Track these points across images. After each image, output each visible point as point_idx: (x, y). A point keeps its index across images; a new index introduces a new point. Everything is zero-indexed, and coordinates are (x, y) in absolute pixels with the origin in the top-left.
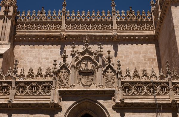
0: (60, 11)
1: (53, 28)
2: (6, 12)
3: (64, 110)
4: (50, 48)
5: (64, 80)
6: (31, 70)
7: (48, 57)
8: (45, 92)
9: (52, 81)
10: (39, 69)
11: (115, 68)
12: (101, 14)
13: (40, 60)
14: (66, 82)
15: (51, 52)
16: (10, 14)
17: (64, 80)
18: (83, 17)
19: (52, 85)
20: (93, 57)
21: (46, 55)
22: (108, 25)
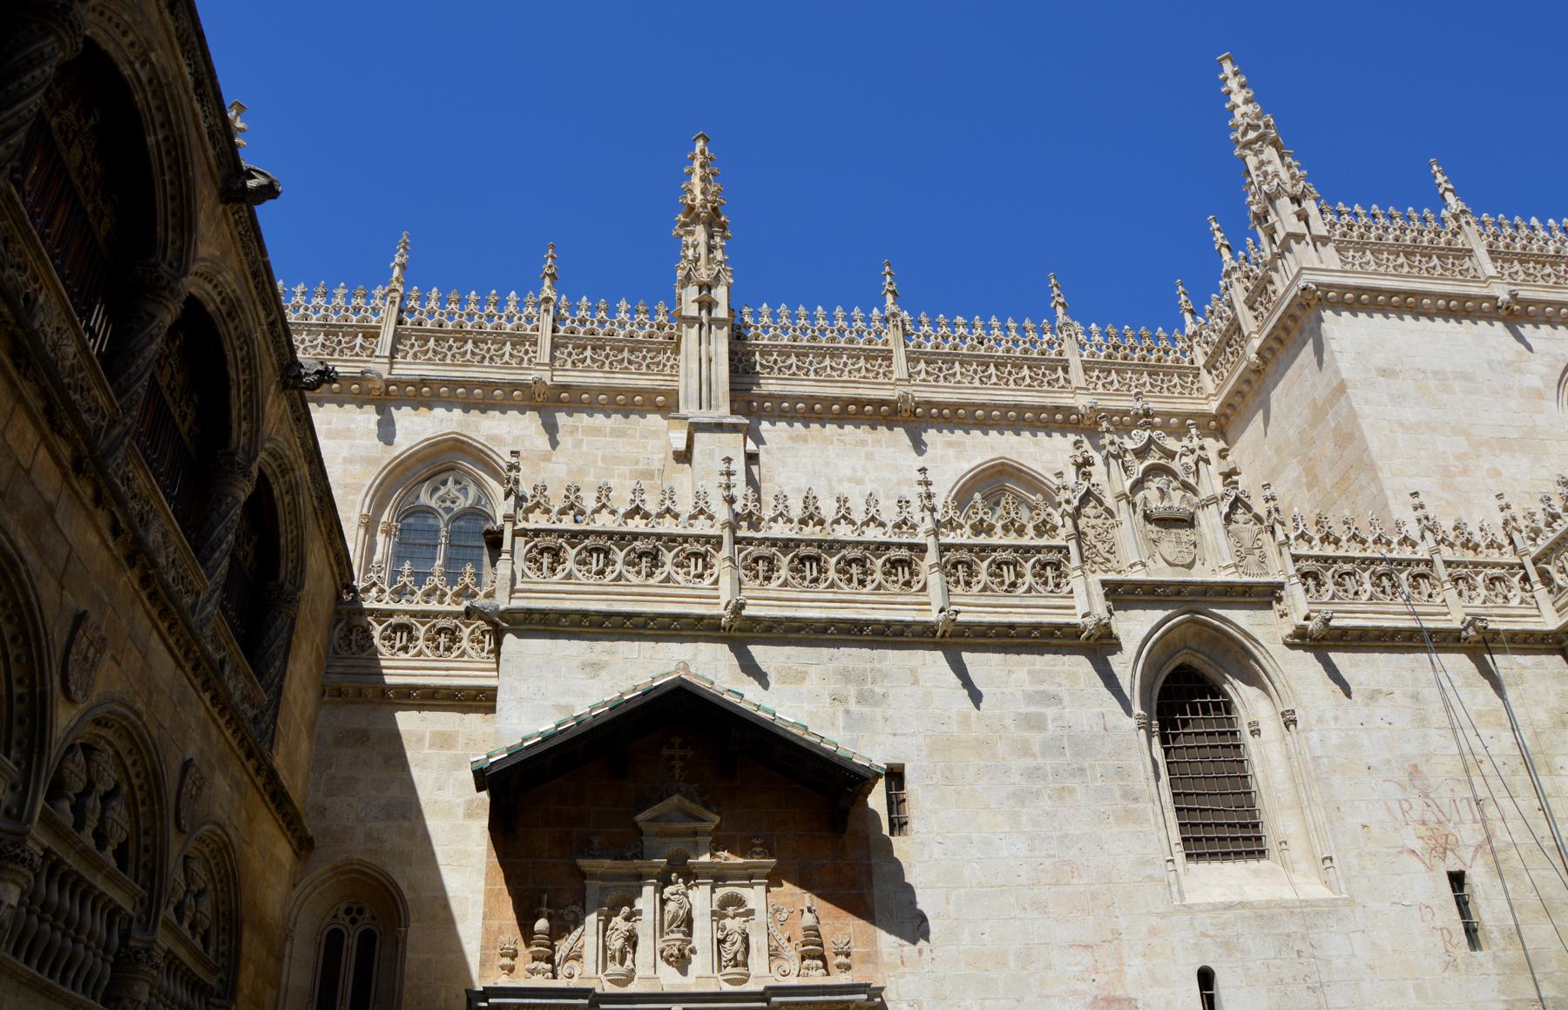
0: (875, 311)
1: (863, 372)
2: (707, 305)
3: (1130, 646)
4: (864, 443)
5: (1099, 545)
7: (860, 474)
8: (1045, 583)
9: (1067, 548)
11: (1260, 508)
12: (1022, 331)
13: (835, 483)
15: (869, 457)
16: (721, 312)
17: (1099, 545)
18: (963, 338)
19: (1068, 560)
20: (1175, 465)
21: (854, 470)
22: (1055, 370)
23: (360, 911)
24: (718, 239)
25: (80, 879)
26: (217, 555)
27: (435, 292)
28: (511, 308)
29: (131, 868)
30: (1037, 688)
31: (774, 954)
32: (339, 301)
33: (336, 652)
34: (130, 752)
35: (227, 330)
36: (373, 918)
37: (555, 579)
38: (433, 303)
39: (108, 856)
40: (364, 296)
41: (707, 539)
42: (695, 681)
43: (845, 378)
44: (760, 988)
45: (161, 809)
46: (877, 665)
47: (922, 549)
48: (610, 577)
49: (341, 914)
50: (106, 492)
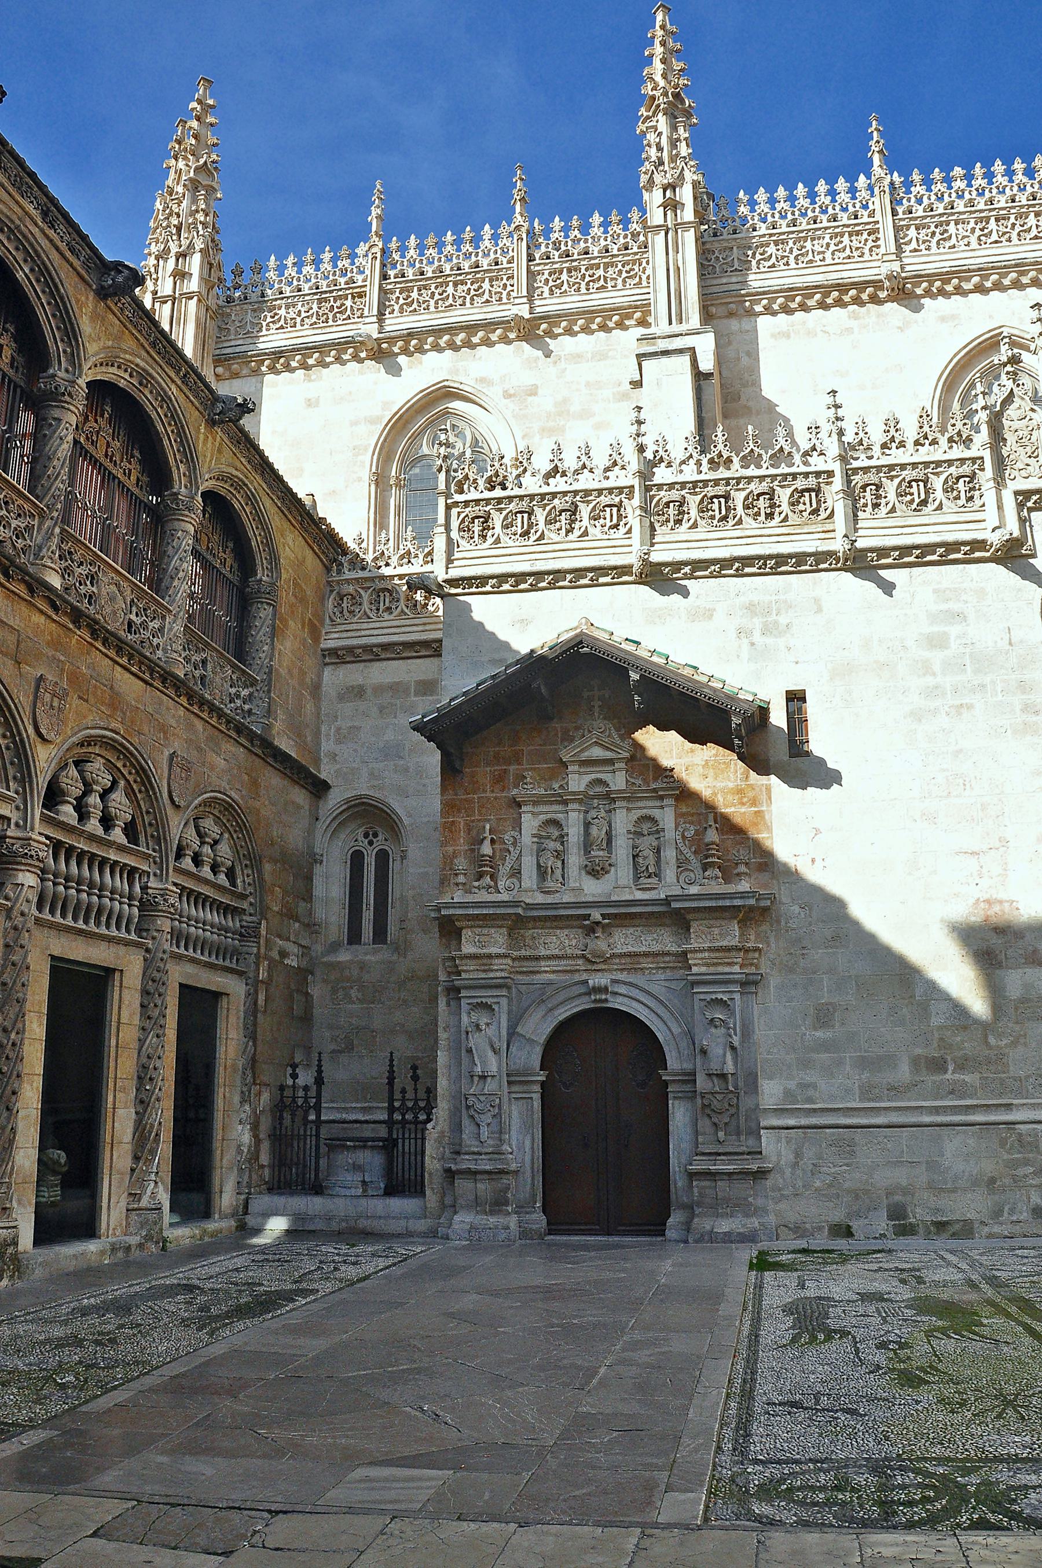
2: (672, 205)
4: (849, 330)
6: (892, 424)
8: (957, 498)
10: (921, 417)
14: (1030, 457)
19: (983, 470)
23: (375, 835)
24: (681, 130)
25: (93, 856)
26: (176, 583)
27: (413, 241)
28: (487, 243)
29: (142, 839)
30: (945, 607)
31: (682, 864)
32: (326, 266)
33: (333, 621)
34: (118, 758)
35: (147, 399)
36: (386, 840)
37: (486, 545)
38: (412, 252)
39: (118, 835)
40: (349, 256)
41: (621, 489)
42: (596, 634)
43: (829, 261)
45: (155, 794)
46: (782, 597)
47: (830, 474)
48: (533, 538)
49: (361, 838)
50: (35, 584)
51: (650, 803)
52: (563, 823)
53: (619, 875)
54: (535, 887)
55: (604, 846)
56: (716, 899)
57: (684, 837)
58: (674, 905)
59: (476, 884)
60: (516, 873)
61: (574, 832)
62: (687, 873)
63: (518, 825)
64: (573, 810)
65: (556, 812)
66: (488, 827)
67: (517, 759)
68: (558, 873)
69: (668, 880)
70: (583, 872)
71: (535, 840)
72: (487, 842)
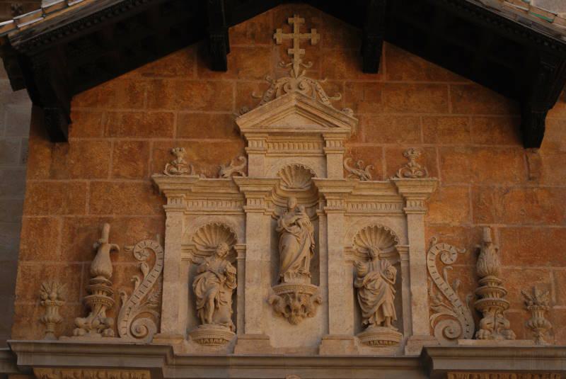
44: (418, 353)
51: (382, 208)
52: (238, 231)
53: (333, 318)
54: (183, 332)
55: (307, 270)
56: (512, 357)
57: (440, 264)
58: (438, 365)
59: (81, 321)
60: (156, 310)
61: (257, 248)
62: (442, 324)
63: (159, 228)
64: (258, 211)
65: (226, 213)
66: (107, 228)
67: (159, 127)
68: (226, 311)
69: (415, 330)
70: (269, 312)
71: (189, 255)
72: (105, 251)
